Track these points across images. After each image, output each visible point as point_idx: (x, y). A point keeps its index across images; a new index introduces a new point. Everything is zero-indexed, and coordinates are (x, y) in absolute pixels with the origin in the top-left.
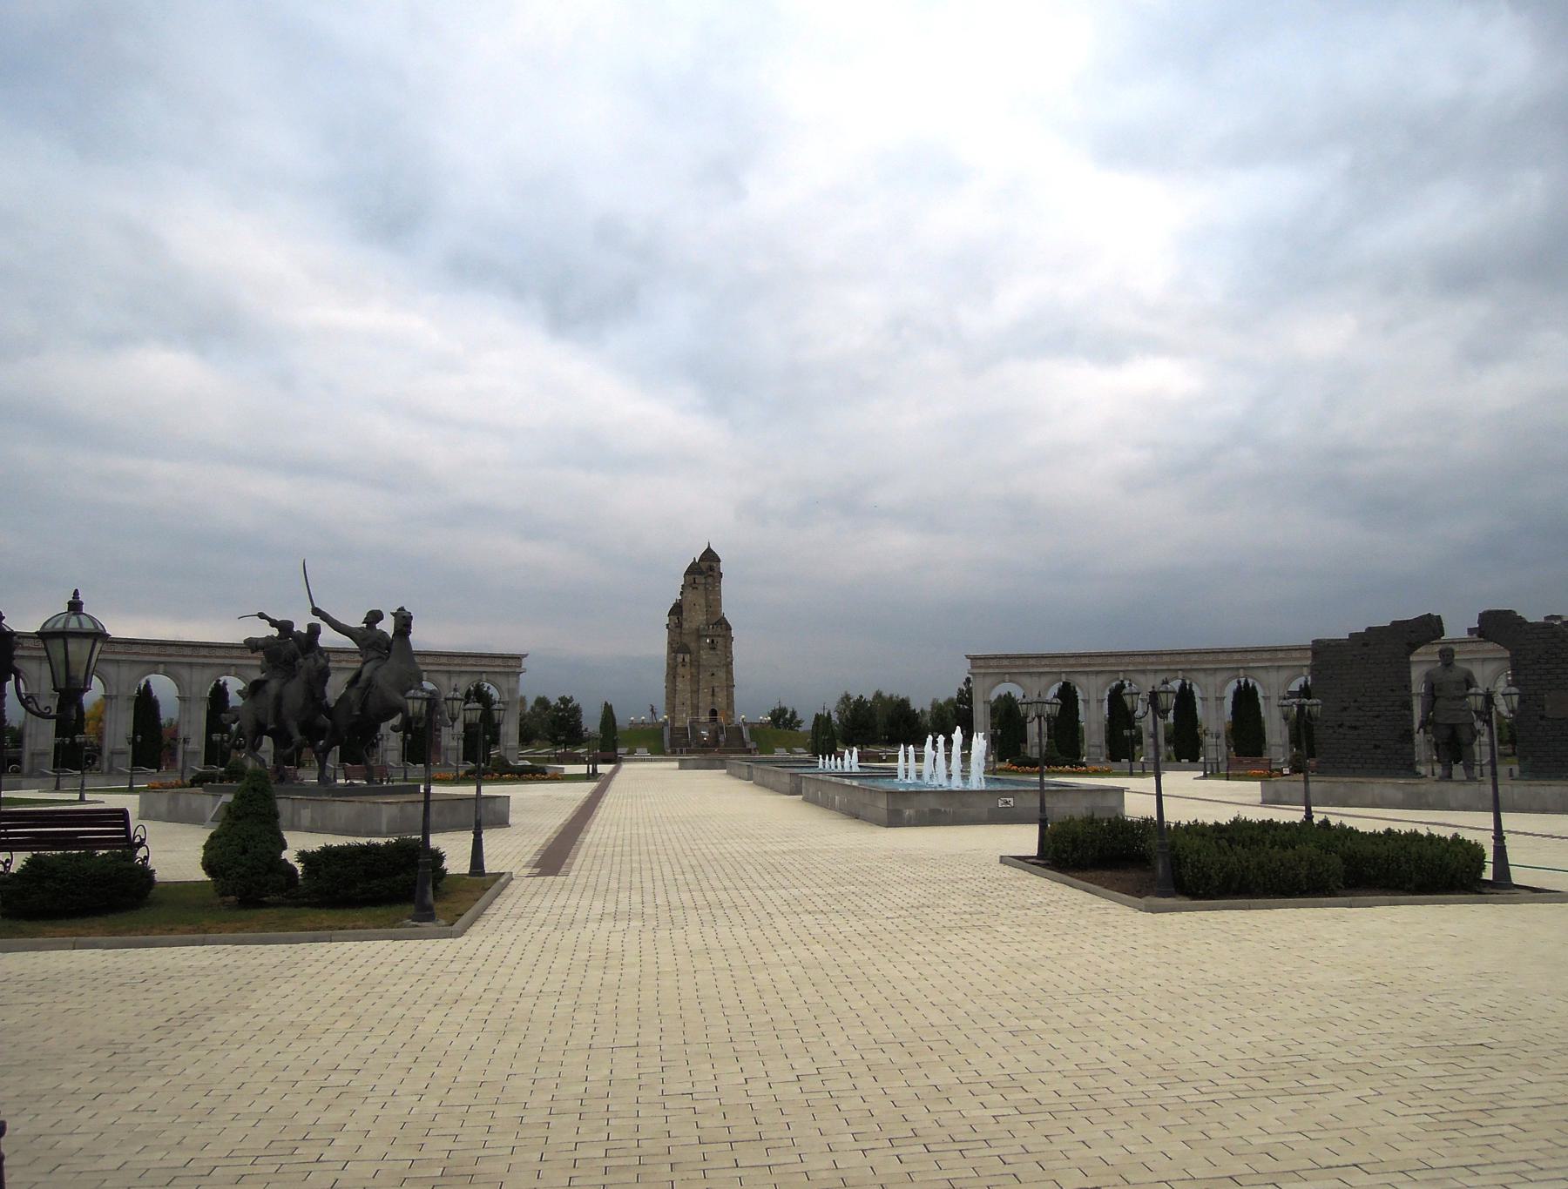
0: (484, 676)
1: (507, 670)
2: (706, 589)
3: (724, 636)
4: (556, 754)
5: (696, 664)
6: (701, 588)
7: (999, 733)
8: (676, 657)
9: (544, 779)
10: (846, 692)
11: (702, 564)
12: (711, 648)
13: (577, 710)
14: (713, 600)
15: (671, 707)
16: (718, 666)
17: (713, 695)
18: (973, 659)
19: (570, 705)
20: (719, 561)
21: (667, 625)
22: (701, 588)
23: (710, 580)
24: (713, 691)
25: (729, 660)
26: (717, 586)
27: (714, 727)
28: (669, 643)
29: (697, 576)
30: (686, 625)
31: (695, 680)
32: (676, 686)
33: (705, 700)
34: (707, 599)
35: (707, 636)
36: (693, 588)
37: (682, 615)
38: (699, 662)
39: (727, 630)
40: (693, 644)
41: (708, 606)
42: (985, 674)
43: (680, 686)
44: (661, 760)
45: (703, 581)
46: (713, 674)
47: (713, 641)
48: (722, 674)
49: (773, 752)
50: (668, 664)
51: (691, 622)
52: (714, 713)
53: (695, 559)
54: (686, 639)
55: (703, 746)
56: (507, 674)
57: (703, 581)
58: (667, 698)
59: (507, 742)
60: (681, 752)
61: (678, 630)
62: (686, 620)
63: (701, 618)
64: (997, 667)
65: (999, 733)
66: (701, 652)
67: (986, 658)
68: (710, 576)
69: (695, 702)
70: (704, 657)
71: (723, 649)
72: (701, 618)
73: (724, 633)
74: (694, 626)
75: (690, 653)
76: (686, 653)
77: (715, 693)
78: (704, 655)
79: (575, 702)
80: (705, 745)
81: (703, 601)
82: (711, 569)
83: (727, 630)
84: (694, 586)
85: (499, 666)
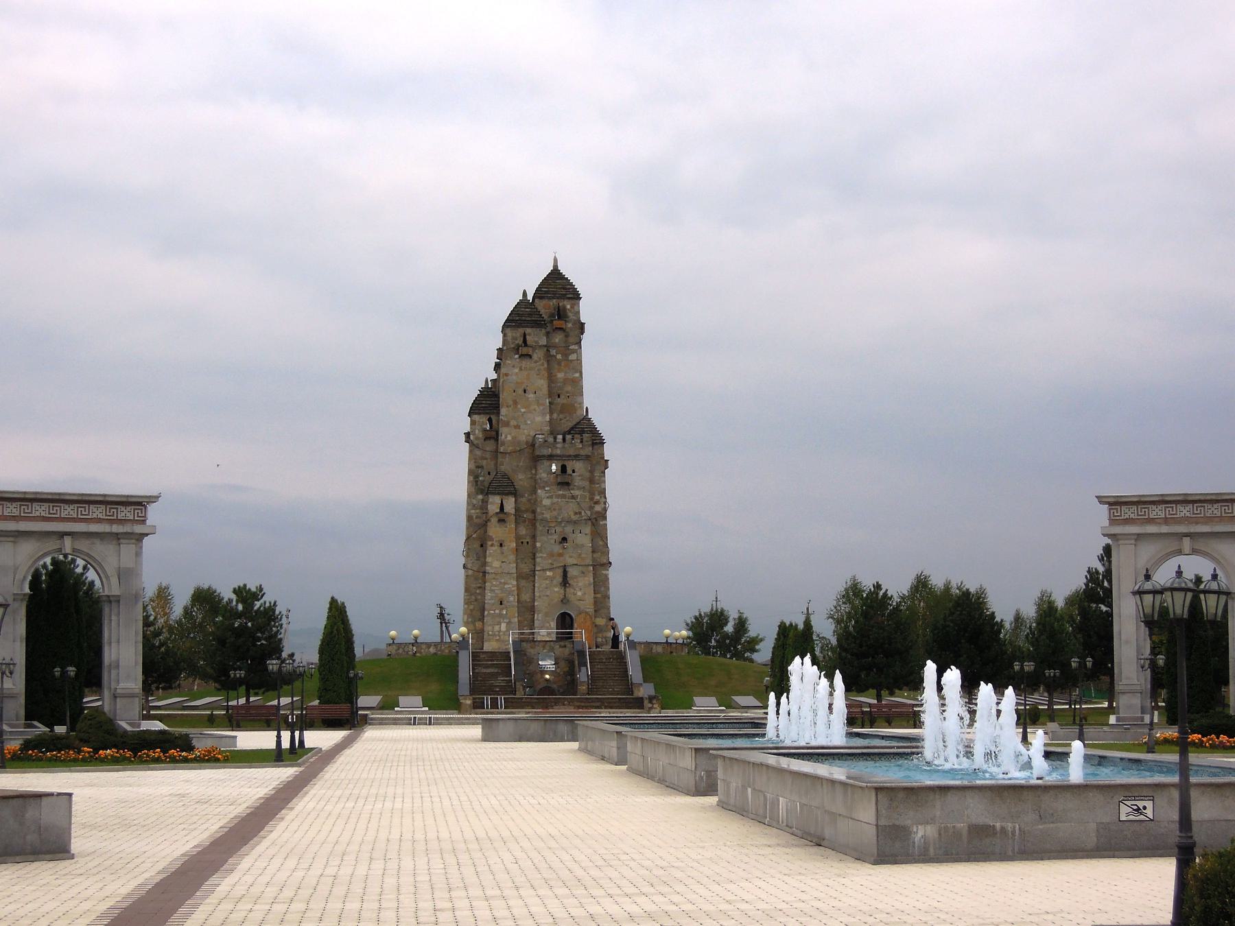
0: (68, 541)
1: (116, 528)
2: (549, 358)
3: (588, 457)
4: (227, 708)
5: (528, 517)
6: (538, 355)
7: (1089, 665)
8: (485, 502)
9: (186, 760)
10: (854, 579)
11: (540, 305)
12: (559, 484)
13: (270, 616)
14: (566, 381)
15: (476, 610)
16: (575, 522)
17: (565, 582)
18: (1115, 503)
19: (258, 604)
20: (576, 296)
21: (468, 435)
22: (538, 355)
23: (558, 338)
25: (598, 508)
26: (574, 351)
27: (567, 651)
28: (470, 472)
29: (528, 330)
30: (506, 435)
31: (527, 551)
32: (485, 564)
33: (547, 593)
34: (551, 379)
35: (551, 458)
36: (522, 356)
37: (498, 413)
38: (534, 512)
39: (593, 444)
40: (521, 476)
41: (554, 394)
42: (1139, 537)
43: (494, 562)
44: (449, 722)
45: (543, 341)
46: (564, 539)
47: (564, 469)
48: (583, 538)
49: (689, 705)
50: (469, 518)
51: (517, 427)
52: (565, 621)
53: (525, 294)
54: (506, 465)
55: (542, 692)
56: (117, 537)
57: (543, 341)
58: (467, 590)
59: (118, 682)
60: (494, 705)
61: (490, 445)
62: (507, 424)
63: (539, 419)
64: (1166, 521)
65: (1089, 665)
66: (539, 491)
67: (1141, 502)
68: (561, 329)
69: (526, 597)
70: (546, 502)
71: (587, 484)
72: (539, 419)
73: (588, 451)
74: (524, 435)
75: (514, 493)
76: (507, 494)
78: (546, 498)
79: (268, 598)
80: (547, 690)
81: (542, 384)
82: (561, 314)
83: (593, 444)
84: (524, 350)
85: (99, 521)
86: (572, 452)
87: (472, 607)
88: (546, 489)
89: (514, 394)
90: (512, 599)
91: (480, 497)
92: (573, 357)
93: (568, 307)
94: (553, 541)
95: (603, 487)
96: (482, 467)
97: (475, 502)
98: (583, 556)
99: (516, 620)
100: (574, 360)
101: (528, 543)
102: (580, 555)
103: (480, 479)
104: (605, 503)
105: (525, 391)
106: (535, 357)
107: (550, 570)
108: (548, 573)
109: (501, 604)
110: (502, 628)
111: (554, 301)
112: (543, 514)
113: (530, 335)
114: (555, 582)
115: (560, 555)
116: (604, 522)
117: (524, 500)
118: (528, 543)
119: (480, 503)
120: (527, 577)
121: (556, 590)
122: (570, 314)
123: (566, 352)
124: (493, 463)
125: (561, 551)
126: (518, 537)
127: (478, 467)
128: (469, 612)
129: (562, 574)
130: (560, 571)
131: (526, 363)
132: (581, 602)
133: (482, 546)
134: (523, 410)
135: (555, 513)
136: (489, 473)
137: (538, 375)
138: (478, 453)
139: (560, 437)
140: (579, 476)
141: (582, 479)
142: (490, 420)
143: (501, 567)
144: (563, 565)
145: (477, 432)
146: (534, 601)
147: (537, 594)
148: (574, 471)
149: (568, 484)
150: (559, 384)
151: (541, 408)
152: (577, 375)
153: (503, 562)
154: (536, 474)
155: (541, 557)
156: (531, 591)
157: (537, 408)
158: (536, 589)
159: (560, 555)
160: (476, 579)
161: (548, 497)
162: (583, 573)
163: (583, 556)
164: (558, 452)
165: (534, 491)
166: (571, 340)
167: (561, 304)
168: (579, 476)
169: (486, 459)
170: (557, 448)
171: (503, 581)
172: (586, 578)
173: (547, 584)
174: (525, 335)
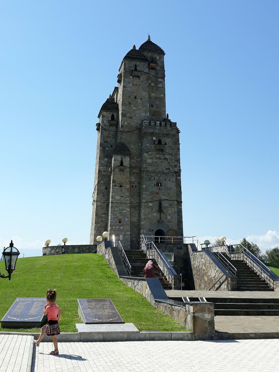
11: (145, 54)
14: (156, 98)
16: (166, 174)
17: (160, 210)
20: (161, 53)
21: (98, 125)
22: (143, 78)
24: (160, 204)
26: (161, 82)
29: (138, 63)
35: (152, 134)
38: (140, 168)
51: (131, 118)
53: (134, 47)
54: (124, 138)
69: (135, 220)
70: (149, 161)
72: (143, 114)
74: (135, 122)
77: (164, 210)
78: (149, 158)
84: (136, 73)
86: (165, 132)
87: (99, 225)
88: (149, 153)
89: (130, 99)
90: (127, 219)
91: (106, 159)
92: (160, 85)
93: (158, 58)
94: (153, 185)
95: (178, 157)
96: (107, 142)
97: (103, 162)
98: (171, 195)
99: (129, 233)
100: (160, 87)
101: (136, 186)
102: (169, 194)
103: (107, 149)
104: (180, 167)
105: (135, 98)
106: (141, 78)
107: (151, 202)
108: (150, 204)
109: (120, 222)
110: (120, 238)
111: (150, 54)
112: (147, 168)
113: (139, 66)
114: (154, 210)
115: (157, 193)
116: (179, 178)
117: (134, 160)
118: (136, 186)
119: (106, 163)
120: (137, 207)
121: (154, 215)
122: (158, 62)
123: (157, 83)
124: (114, 140)
125: (158, 191)
126: (131, 182)
127: (105, 142)
128: (97, 228)
129: (158, 205)
130: (158, 203)
131: (136, 81)
132: (170, 223)
133: (106, 189)
134: (134, 108)
135: (154, 168)
136: (112, 146)
137: (143, 89)
138: (106, 134)
139: (158, 122)
140: (169, 147)
141: (170, 149)
142: (113, 117)
143: (120, 199)
144: (159, 199)
145: (105, 121)
146: (139, 220)
147: (143, 217)
148: (166, 144)
149: (162, 151)
150: (152, 100)
151: (145, 108)
152: (163, 95)
153: (122, 196)
154: (142, 146)
155: (145, 194)
156: (137, 215)
157: (142, 108)
158: (142, 214)
159: (157, 193)
160: (102, 208)
161: (150, 158)
162: (171, 205)
163: (171, 195)
164: (157, 131)
165: (140, 155)
166: (159, 76)
167: (154, 56)
168: (169, 147)
169: (110, 137)
170: (156, 129)
171: (121, 208)
172: (173, 209)
173: (149, 211)
174: (136, 66)
